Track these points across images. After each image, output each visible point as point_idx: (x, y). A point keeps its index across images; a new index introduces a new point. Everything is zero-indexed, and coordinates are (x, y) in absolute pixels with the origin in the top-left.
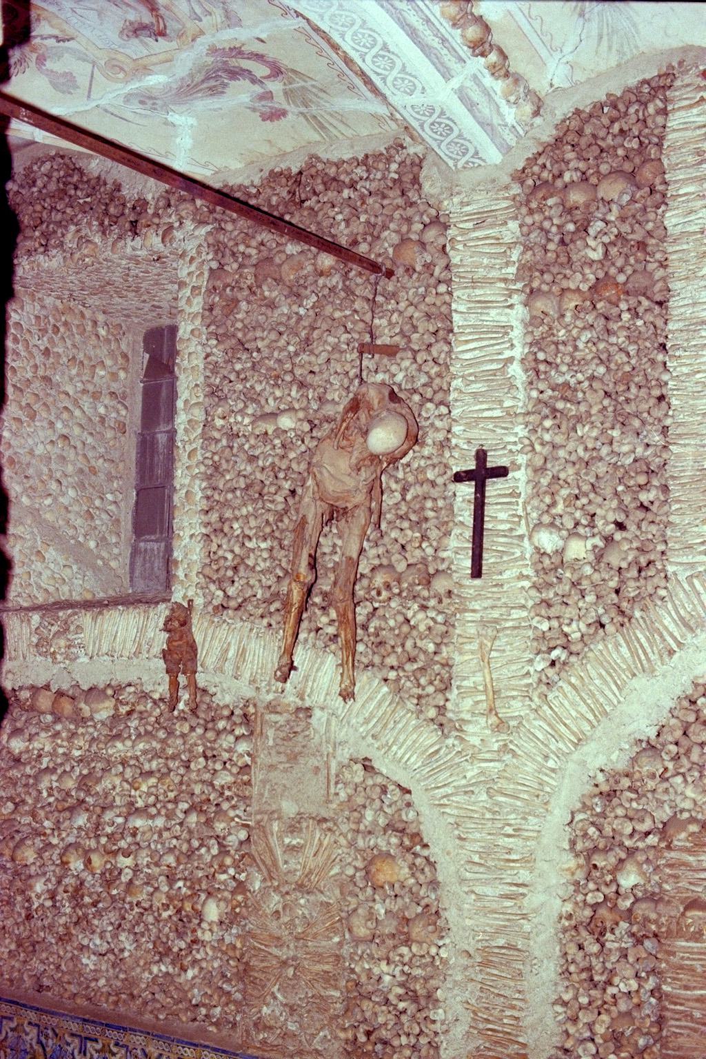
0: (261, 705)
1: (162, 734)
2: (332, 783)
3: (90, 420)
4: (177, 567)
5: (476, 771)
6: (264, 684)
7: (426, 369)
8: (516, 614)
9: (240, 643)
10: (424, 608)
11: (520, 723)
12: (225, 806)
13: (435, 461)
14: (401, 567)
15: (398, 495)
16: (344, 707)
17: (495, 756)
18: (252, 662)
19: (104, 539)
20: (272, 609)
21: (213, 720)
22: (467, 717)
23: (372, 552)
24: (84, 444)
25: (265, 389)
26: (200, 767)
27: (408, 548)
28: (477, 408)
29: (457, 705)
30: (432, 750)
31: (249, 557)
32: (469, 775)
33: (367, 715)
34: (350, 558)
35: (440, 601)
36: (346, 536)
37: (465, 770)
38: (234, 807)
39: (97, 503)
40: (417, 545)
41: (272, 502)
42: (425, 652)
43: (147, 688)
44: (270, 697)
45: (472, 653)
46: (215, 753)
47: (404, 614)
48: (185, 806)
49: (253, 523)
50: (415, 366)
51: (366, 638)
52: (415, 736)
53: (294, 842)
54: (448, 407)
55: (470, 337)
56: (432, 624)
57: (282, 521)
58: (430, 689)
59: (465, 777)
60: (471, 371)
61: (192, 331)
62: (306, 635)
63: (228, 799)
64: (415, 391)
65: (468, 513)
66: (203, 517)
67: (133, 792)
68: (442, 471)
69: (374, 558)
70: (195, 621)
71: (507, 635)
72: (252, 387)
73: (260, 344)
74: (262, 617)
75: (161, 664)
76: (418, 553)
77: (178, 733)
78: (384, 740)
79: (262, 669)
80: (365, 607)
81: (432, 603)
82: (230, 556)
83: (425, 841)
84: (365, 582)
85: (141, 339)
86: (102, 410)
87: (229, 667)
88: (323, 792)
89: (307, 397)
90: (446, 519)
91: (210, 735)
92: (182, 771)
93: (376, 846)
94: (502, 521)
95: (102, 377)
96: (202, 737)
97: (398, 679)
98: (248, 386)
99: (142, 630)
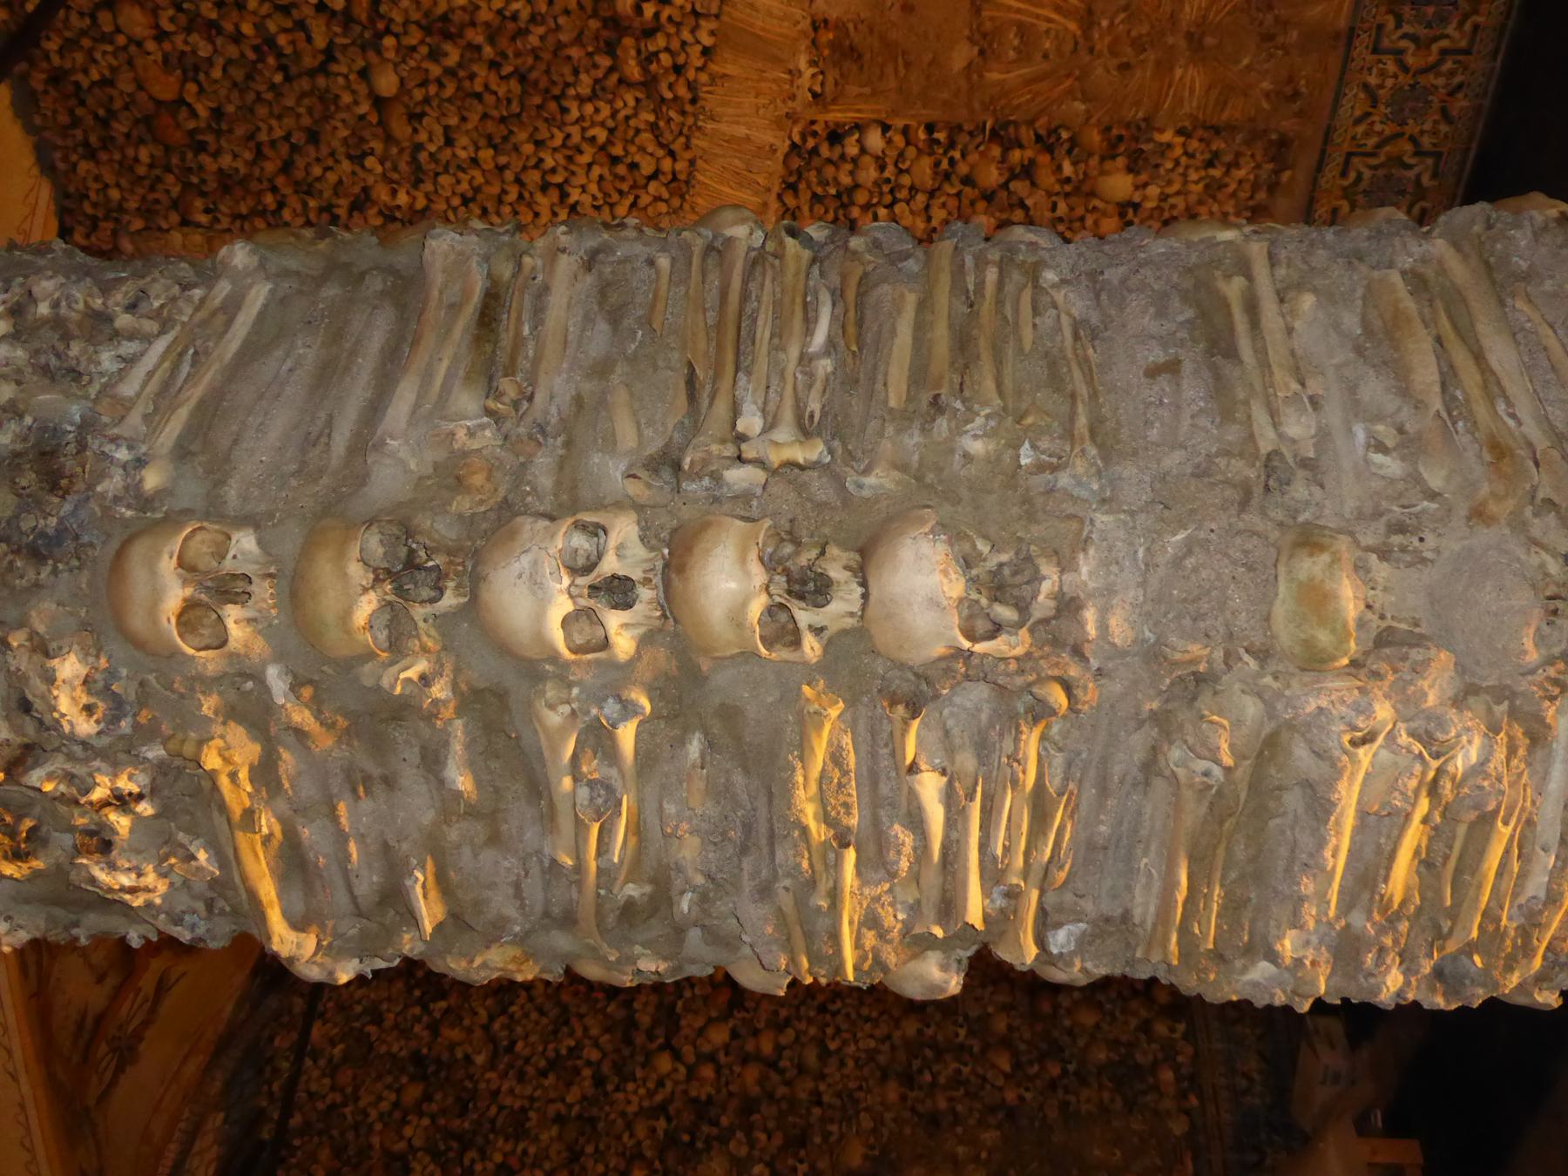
20: (669, 95)
25: (343, 121)
31: (593, 139)
41: (509, 101)
46: (886, 188)
53: (1016, 42)
63: (952, 161)
72: (345, 141)
82: (596, 171)
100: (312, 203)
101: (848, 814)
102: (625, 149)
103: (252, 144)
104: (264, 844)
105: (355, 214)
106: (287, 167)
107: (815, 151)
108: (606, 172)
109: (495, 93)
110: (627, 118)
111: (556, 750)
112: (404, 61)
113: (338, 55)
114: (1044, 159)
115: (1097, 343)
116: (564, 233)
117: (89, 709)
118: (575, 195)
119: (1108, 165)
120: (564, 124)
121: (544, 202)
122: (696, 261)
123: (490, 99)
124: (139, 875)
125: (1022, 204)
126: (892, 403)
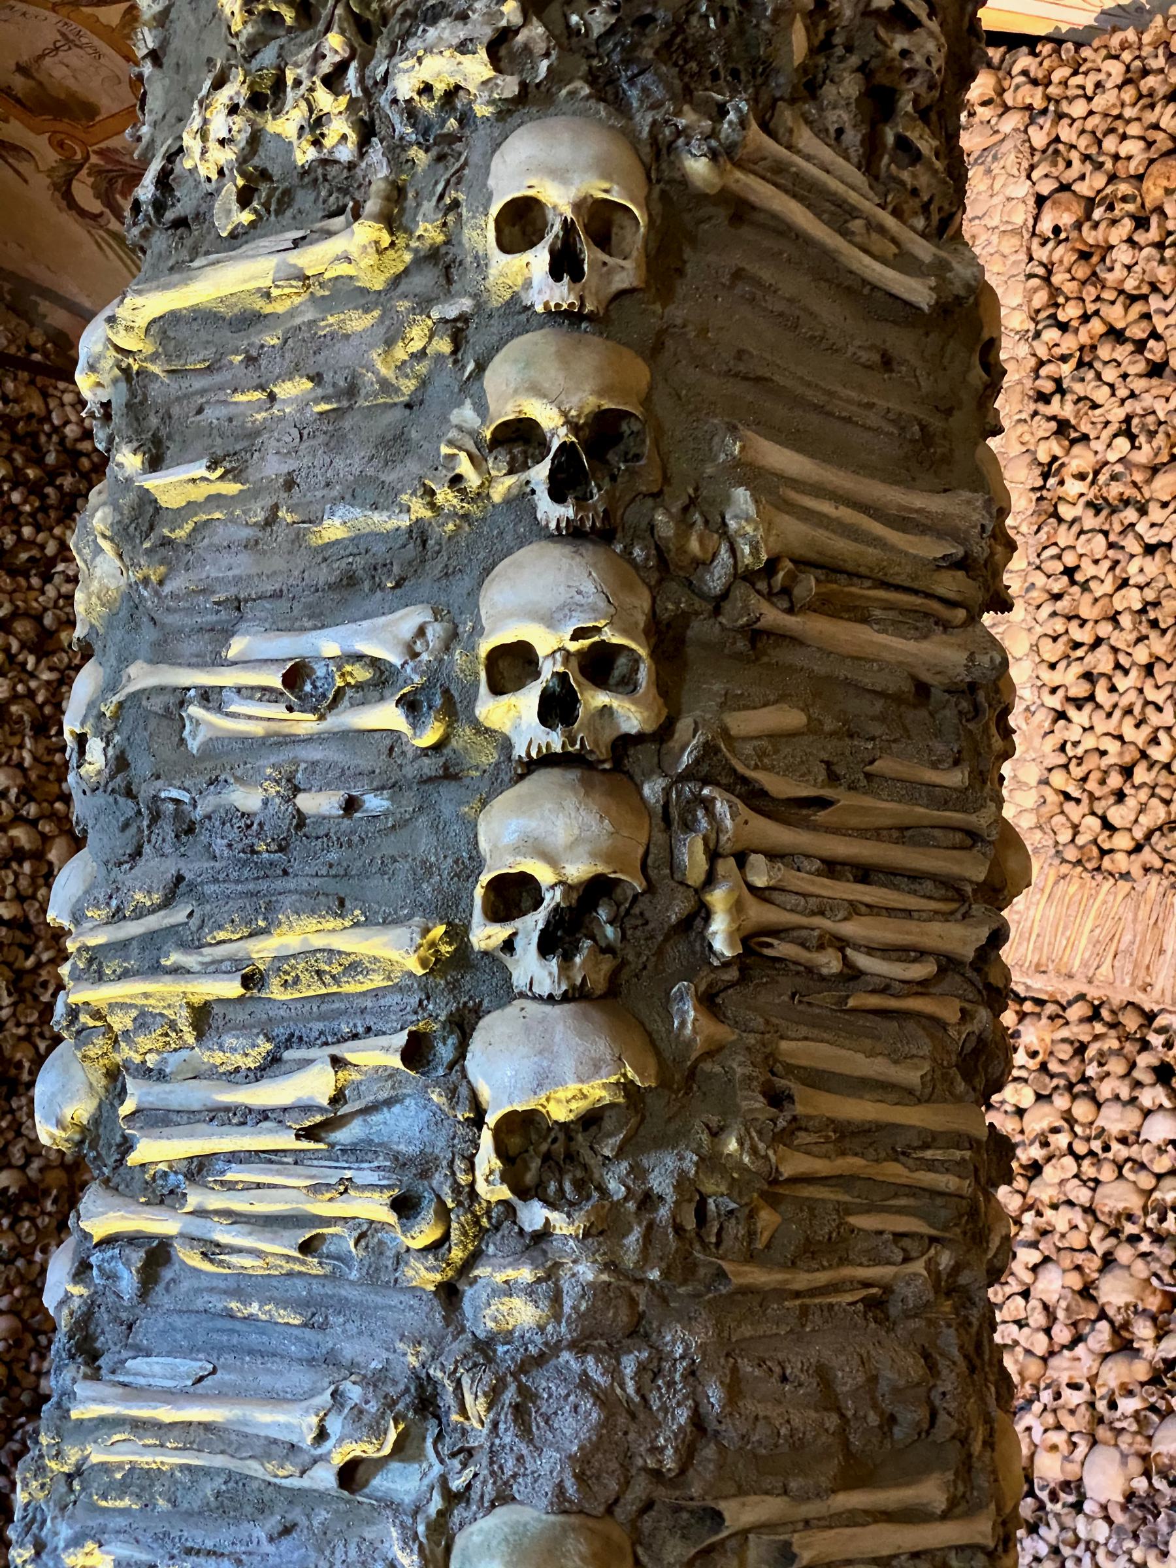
46: (1096, 1146)
63: (1134, 1239)
82: (1112, 746)
100: (1066, 369)
101: (285, 984)
102: (1144, 784)
103: (1145, 290)
104: (259, 290)
105: (1053, 425)
106: (1116, 335)
107: (1145, 1046)
111: (370, 635)
114: (1141, 1371)
115: (860, 1306)
116: (992, 659)
117: (426, 89)
118: (1079, 717)
119: (1135, 1465)
121: (1069, 677)
122: (956, 817)
124: (222, 142)
125: (1078, 1339)
126: (784, 1045)
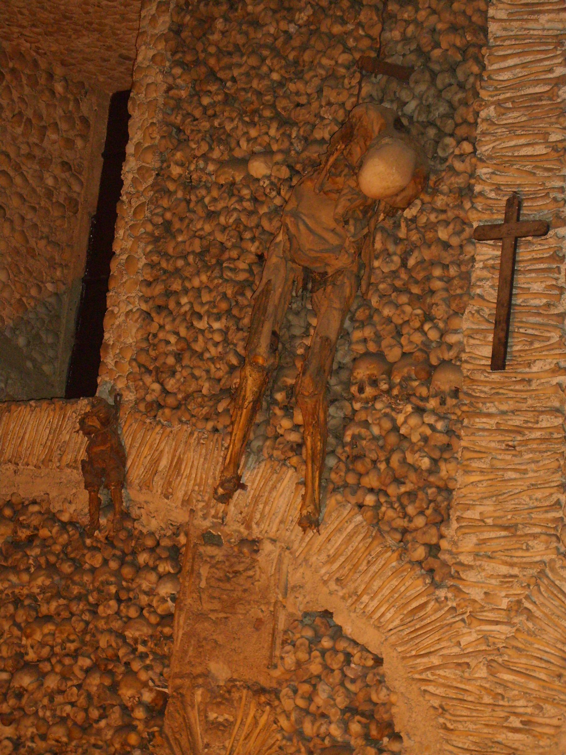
0: (194, 533)
1: (67, 568)
2: (279, 641)
3: (34, 190)
4: (107, 352)
5: (474, 636)
6: (201, 505)
7: (447, 95)
8: (547, 421)
9: (175, 450)
10: (420, 411)
11: (542, 572)
12: (136, 666)
13: (450, 214)
14: (393, 355)
15: (396, 259)
16: (302, 539)
17: (501, 616)
18: (189, 477)
19: (38, 336)
21: (134, 553)
22: (466, 559)
23: (357, 335)
24: (23, 218)
25: (237, 128)
26: (109, 612)
27: (405, 330)
28: (512, 143)
29: (455, 543)
30: (415, 604)
31: (196, 340)
32: (464, 641)
33: (332, 552)
34: (327, 339)
35: (443, 402)
36: (323, 309)
37: (458, 634)
38: (148, 668)
39: (34, 292)
40: (417, 325)
41: (234, 270)
42: (415, 469)
43: (56, 507)
44: (207, 524)
45: (482, 471)
46: (131, 595)
47: (393, 420)
48: (85, 662)
49: (206, 298)
50: (432, 91)
51: (339, 450)
52: (395, 582)
53: (221, 719)
54: (474, 145)
55: (509, 52)
56: (428, 432)
57: (243, 294)
58: (420, 521)
59: (459, 643)
60: (508, 95)
61: (154, 56)
62: (260, 443)
63: (143, 657)
64: (432, 124)
65: (489, 283)
66: (144, 289)
67: (24, 641)
68: (458, 228)
69: (357, 342)
70: (122, 422)
71: (532, 451)
73: (236, 72)
74: (207, 419)
75: (77, 475)
76: (417, 338)
77: (87, 566)
78: (351, 586)
79: (199, 485)
80: (342, 408)
81: (432, 403)
82: (173, 339)
83: (397, 729)
84: (344, 375)
85: (107, 103)
86: (50, 182)
87: (158, 482)
88: (265, 652)
89: (290, 136)
90: (459, 291)
91: (127, 571)
92: (87, 617)
93: (329, 735)
94: (537, 295)
95: (55, 142)
96: (117, 573)
97: (378, 505)
98: (216, 124)
99: (56, 432)
102: (189, 366)
106: (212, 75)
108: (170, 348)
109: (238, 259)
110: (208, 372)
112: (272, 183)
113: (281, 131)
118: (158, 319)
120: (209, 317)
123: (234, 254)
